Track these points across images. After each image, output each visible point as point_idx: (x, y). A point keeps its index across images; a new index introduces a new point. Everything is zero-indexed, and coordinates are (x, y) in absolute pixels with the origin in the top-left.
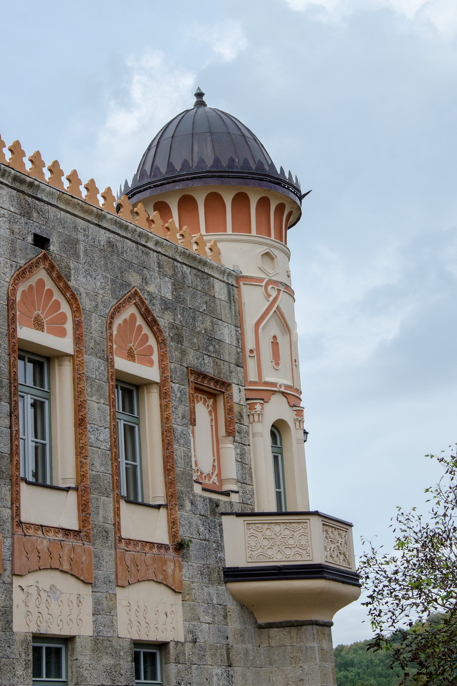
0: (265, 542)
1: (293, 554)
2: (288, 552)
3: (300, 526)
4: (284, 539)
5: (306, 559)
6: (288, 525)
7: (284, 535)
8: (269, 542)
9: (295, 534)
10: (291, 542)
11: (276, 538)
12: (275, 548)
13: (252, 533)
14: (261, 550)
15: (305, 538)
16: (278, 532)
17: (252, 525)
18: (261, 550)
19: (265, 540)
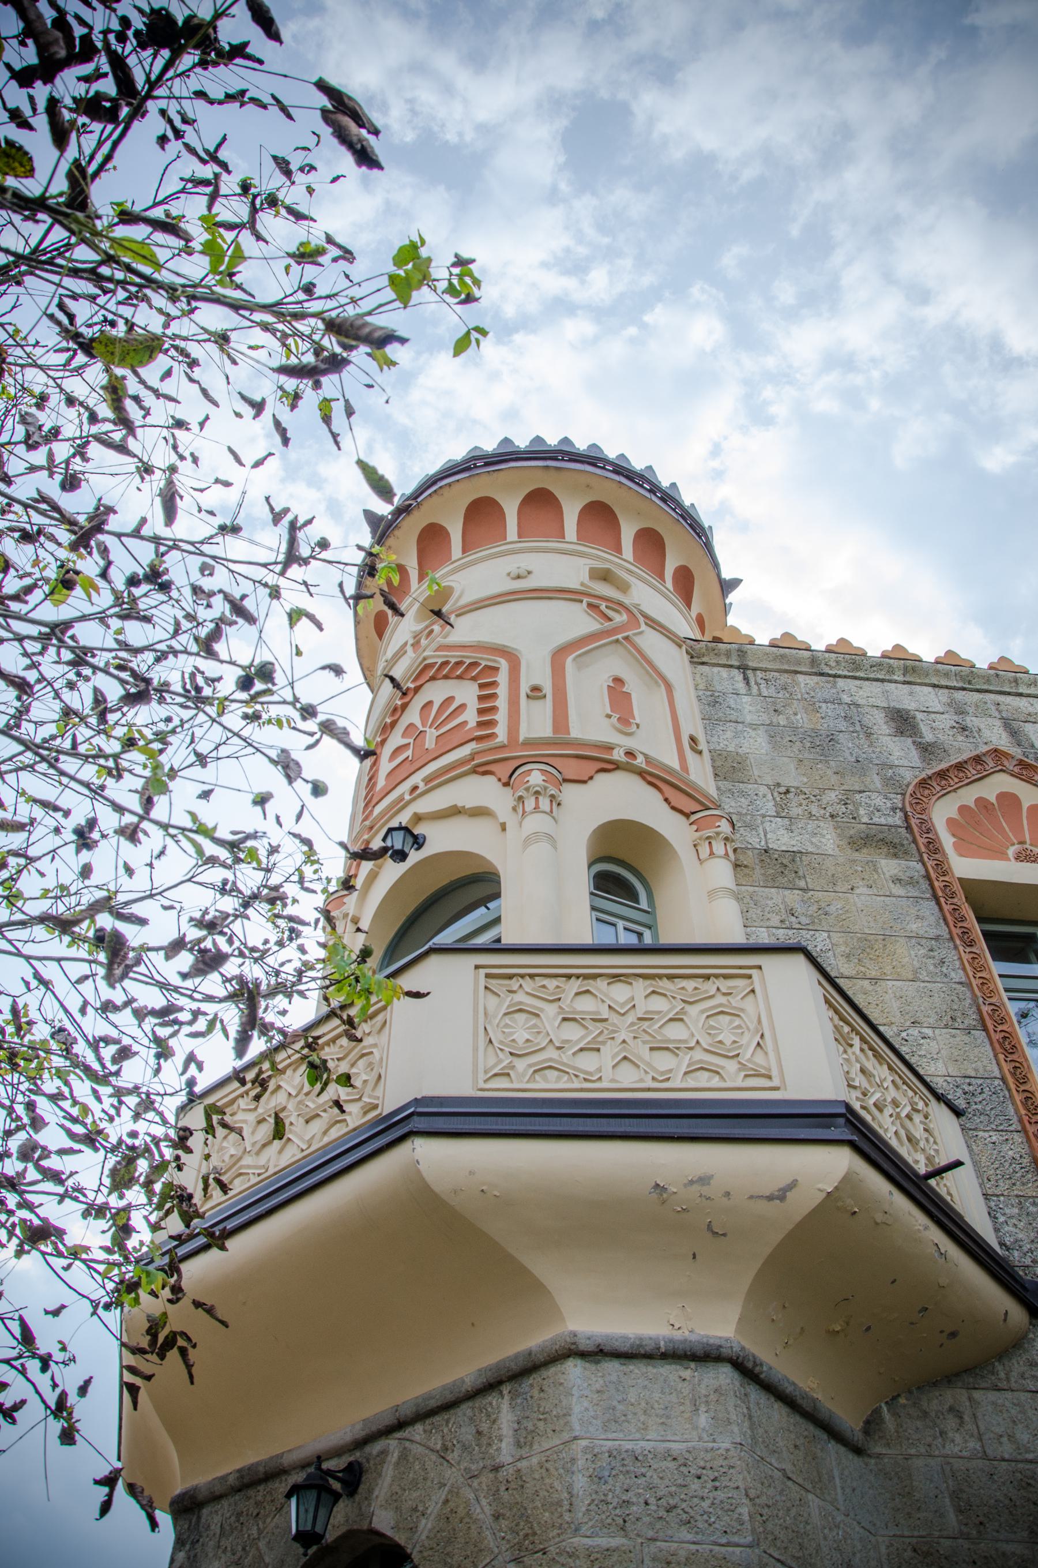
0: (573, 1033)
1: (684, 1069)
2: (664, 1062)
3: (710, 987)
4: (647, 1023)
5: (739, 1083)
6: (665, 984)
7: (647, 1012)
8: (582, 1032)
9: (693, 1010)
10: (675, 1032)
11: (614, 1018)
12: (609, 1052)
13: (521, 1003)
14: (551, 1053)
15: (731, 1022)
16: (622, 1000)
17: (521, 981)
18: (551, 1053)
19: (566, 1023)
